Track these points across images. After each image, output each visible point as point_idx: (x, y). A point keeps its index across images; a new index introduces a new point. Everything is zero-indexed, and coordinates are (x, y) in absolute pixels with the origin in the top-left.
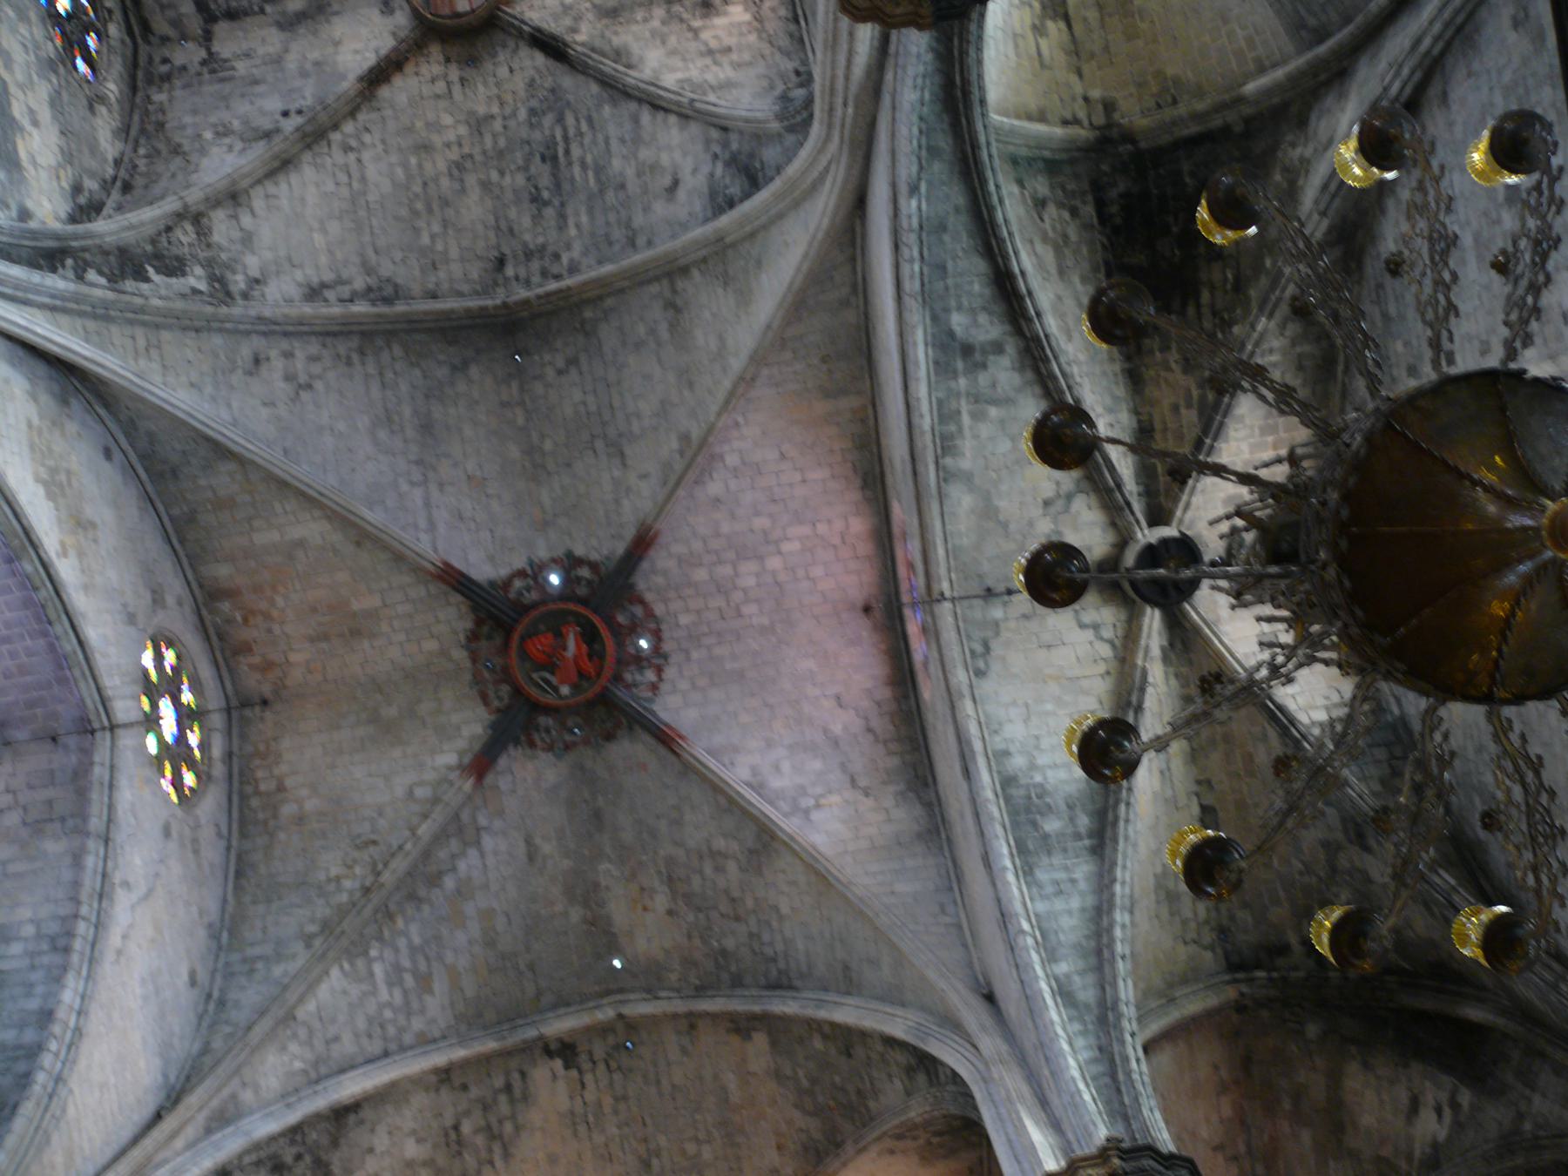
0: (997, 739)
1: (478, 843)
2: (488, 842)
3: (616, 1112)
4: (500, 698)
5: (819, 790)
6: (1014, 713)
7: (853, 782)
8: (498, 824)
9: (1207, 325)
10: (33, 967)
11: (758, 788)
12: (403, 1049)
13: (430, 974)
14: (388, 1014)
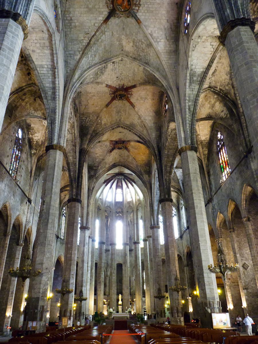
0: (192, 62)
1: (105, 34)
2: (106, 33)
3: (118, 68)
4: (111, 7)
5: (161, 38)
6: (196, 58)
7: (166, 39)
8: (108, 30)
9: (255, 9)
10: (48, 73)
11: (151, 35)
12: (92, 66)
13: (96, 54)
14: (90, 61)
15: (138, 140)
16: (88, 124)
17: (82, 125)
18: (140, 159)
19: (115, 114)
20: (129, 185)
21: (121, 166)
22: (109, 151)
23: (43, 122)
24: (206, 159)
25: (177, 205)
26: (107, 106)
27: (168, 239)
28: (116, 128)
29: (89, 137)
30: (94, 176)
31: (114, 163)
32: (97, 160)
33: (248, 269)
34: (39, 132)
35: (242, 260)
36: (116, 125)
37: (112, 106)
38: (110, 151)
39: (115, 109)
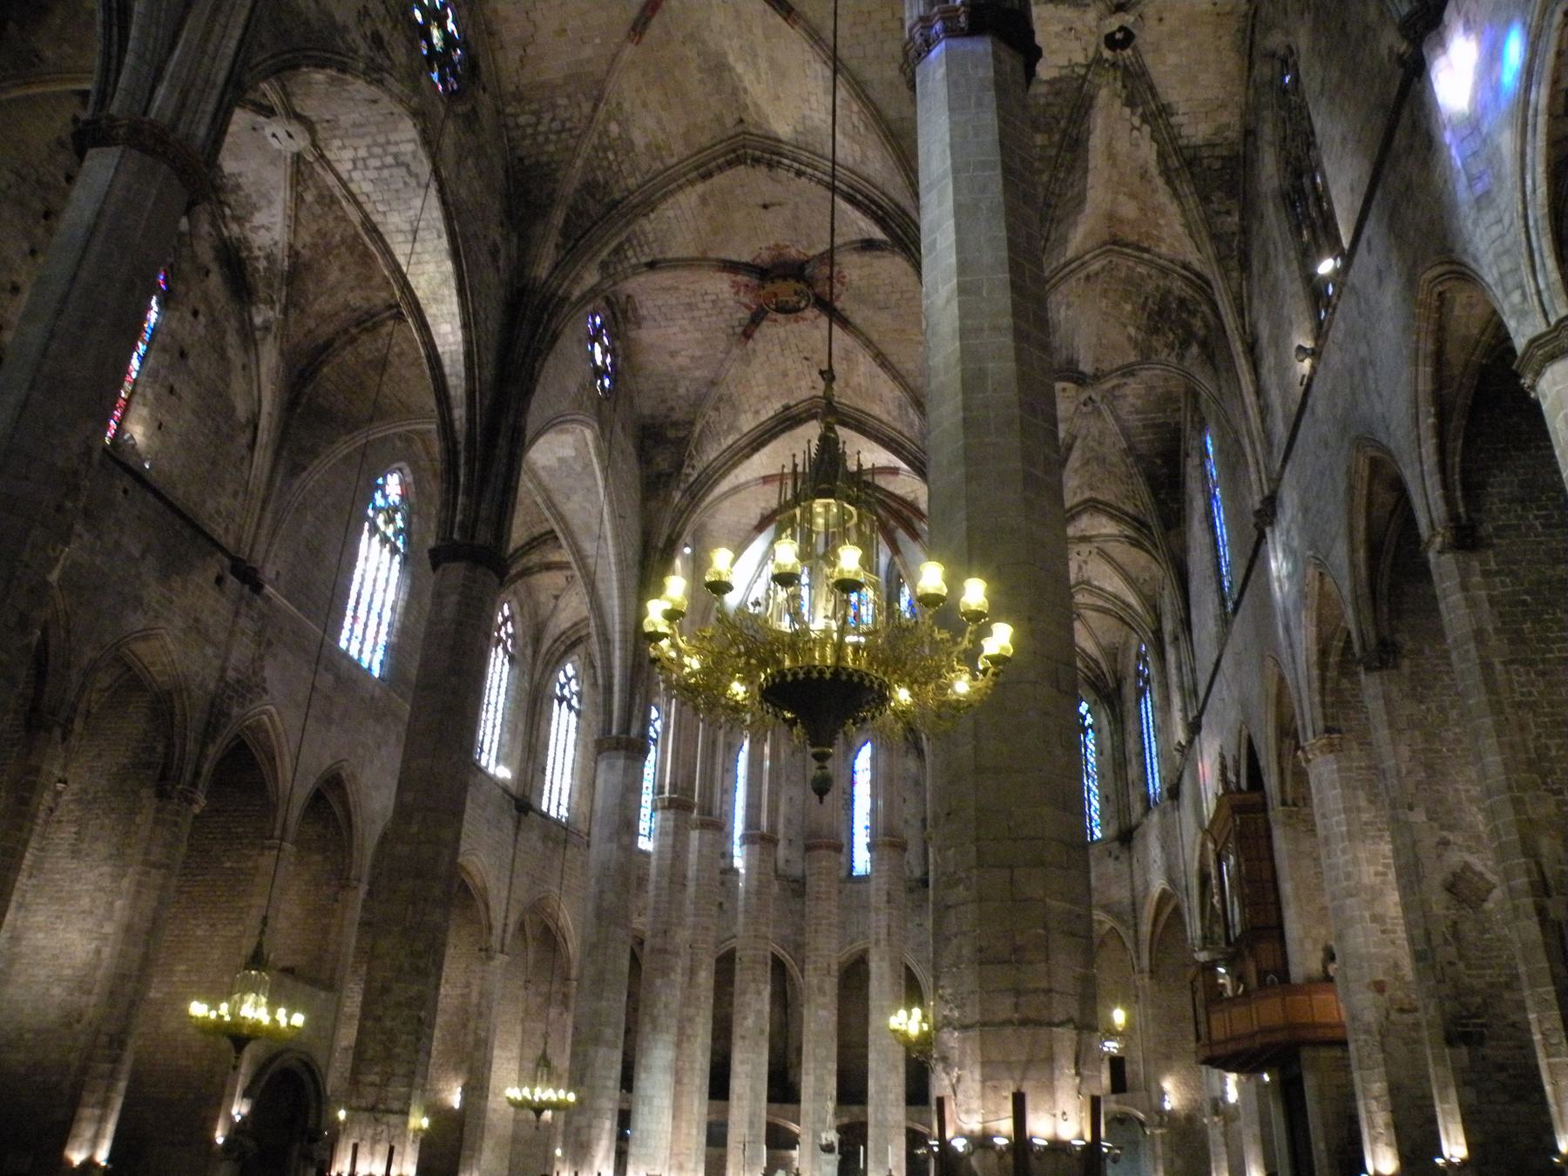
15: (867, 237)
16: (551, 148)
17: (521, 160)
18: (910, 366)
19: (701, 81)
20: (901, 534)
22: (739, 330)
23: (268, 131)
24: (1234, 264)
25: (1149, 619)
26: (638, 28)
28: (720, 169)
29: (558, 217)
30: (670, 475)
31: (787, 408)
32: (682, 391)
33: (1489, 906)
34: (270, 202)
35: (1445, 843)
36: (724, 154)
37: (668, 33)
39: (690, 52)
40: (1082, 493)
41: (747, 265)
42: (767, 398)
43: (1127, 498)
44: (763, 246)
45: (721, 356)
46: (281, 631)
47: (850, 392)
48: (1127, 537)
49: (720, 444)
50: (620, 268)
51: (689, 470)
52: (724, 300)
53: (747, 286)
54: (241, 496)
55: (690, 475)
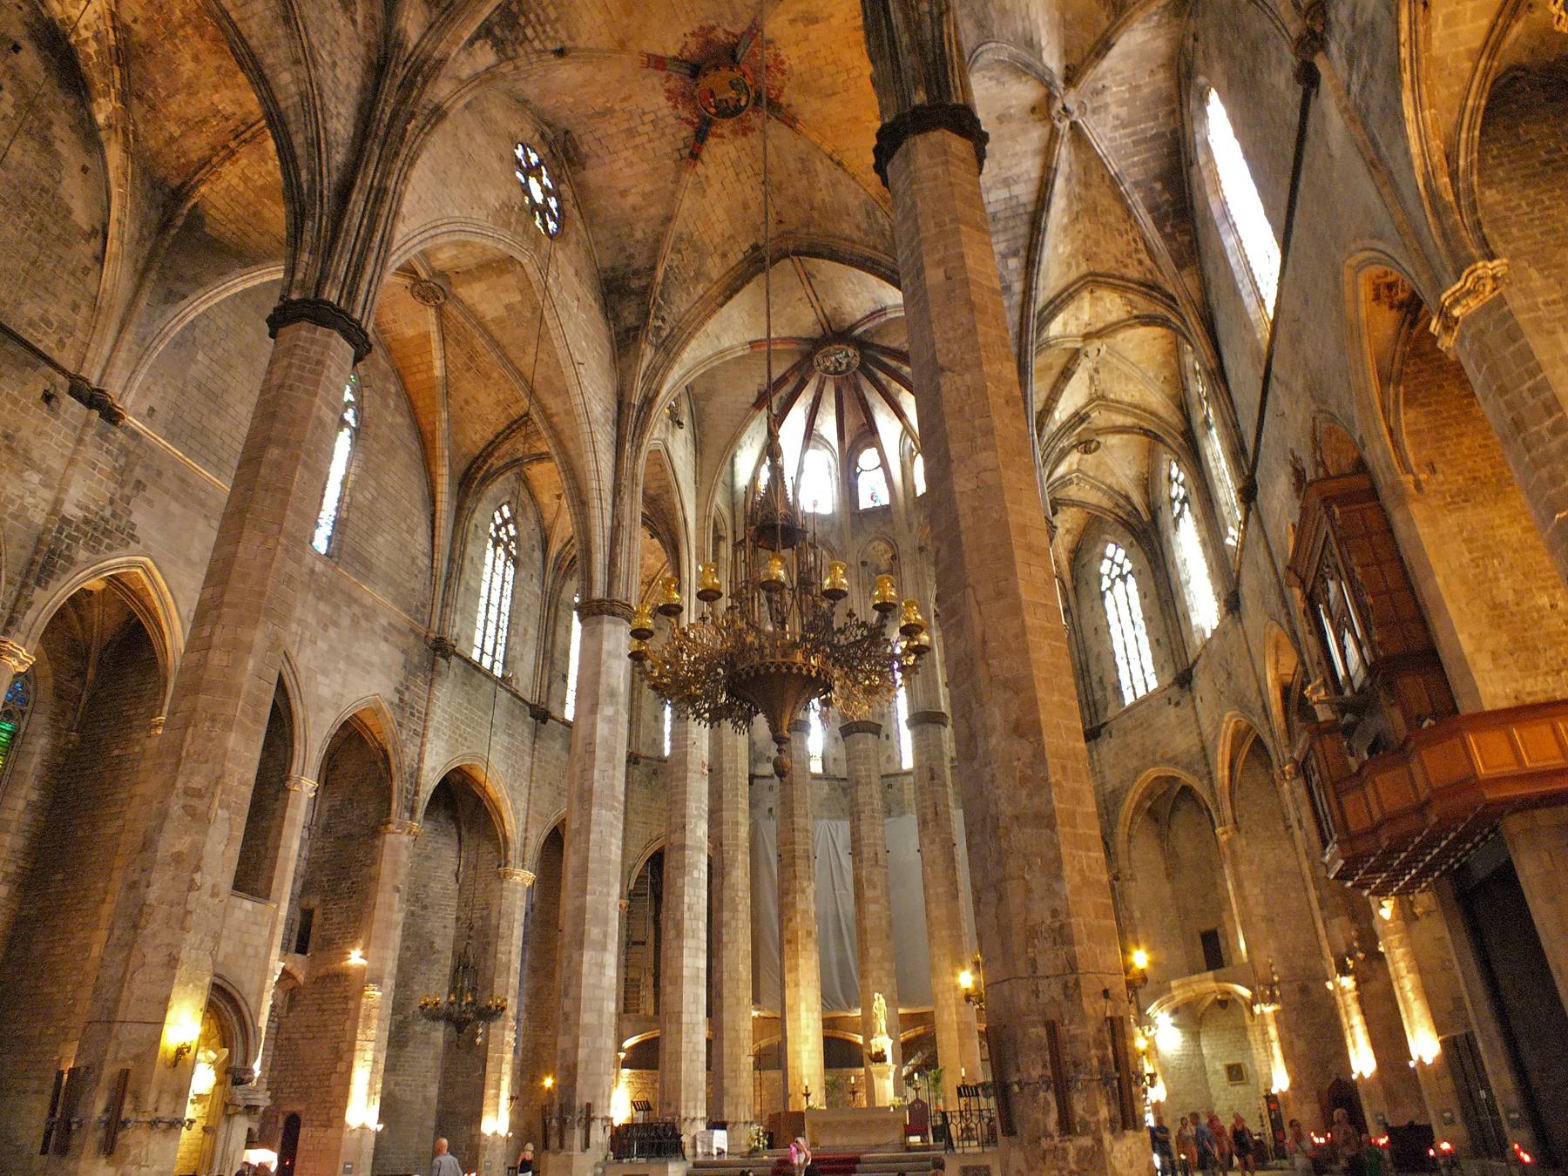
21: (798, 253)
22: (686, 152)
27: (938, 388)
30: (637, 328)
31: (755, 248)
32: (639, 235)
38: (691, 153)
40: (1078, 266)
41: (675, 59)
42: (732, 237)
43: (1129, 256)
44: (688, 30)
45: (671, 186)
46: (159, 474)
47: (816, 215)
48: (1136, 317)
49: (689, 294)
50: (521, 51)
51: (660, 323)
52: (663, 119)
53: (683, 95)
54: (84, 311)
55: (660, 328)
